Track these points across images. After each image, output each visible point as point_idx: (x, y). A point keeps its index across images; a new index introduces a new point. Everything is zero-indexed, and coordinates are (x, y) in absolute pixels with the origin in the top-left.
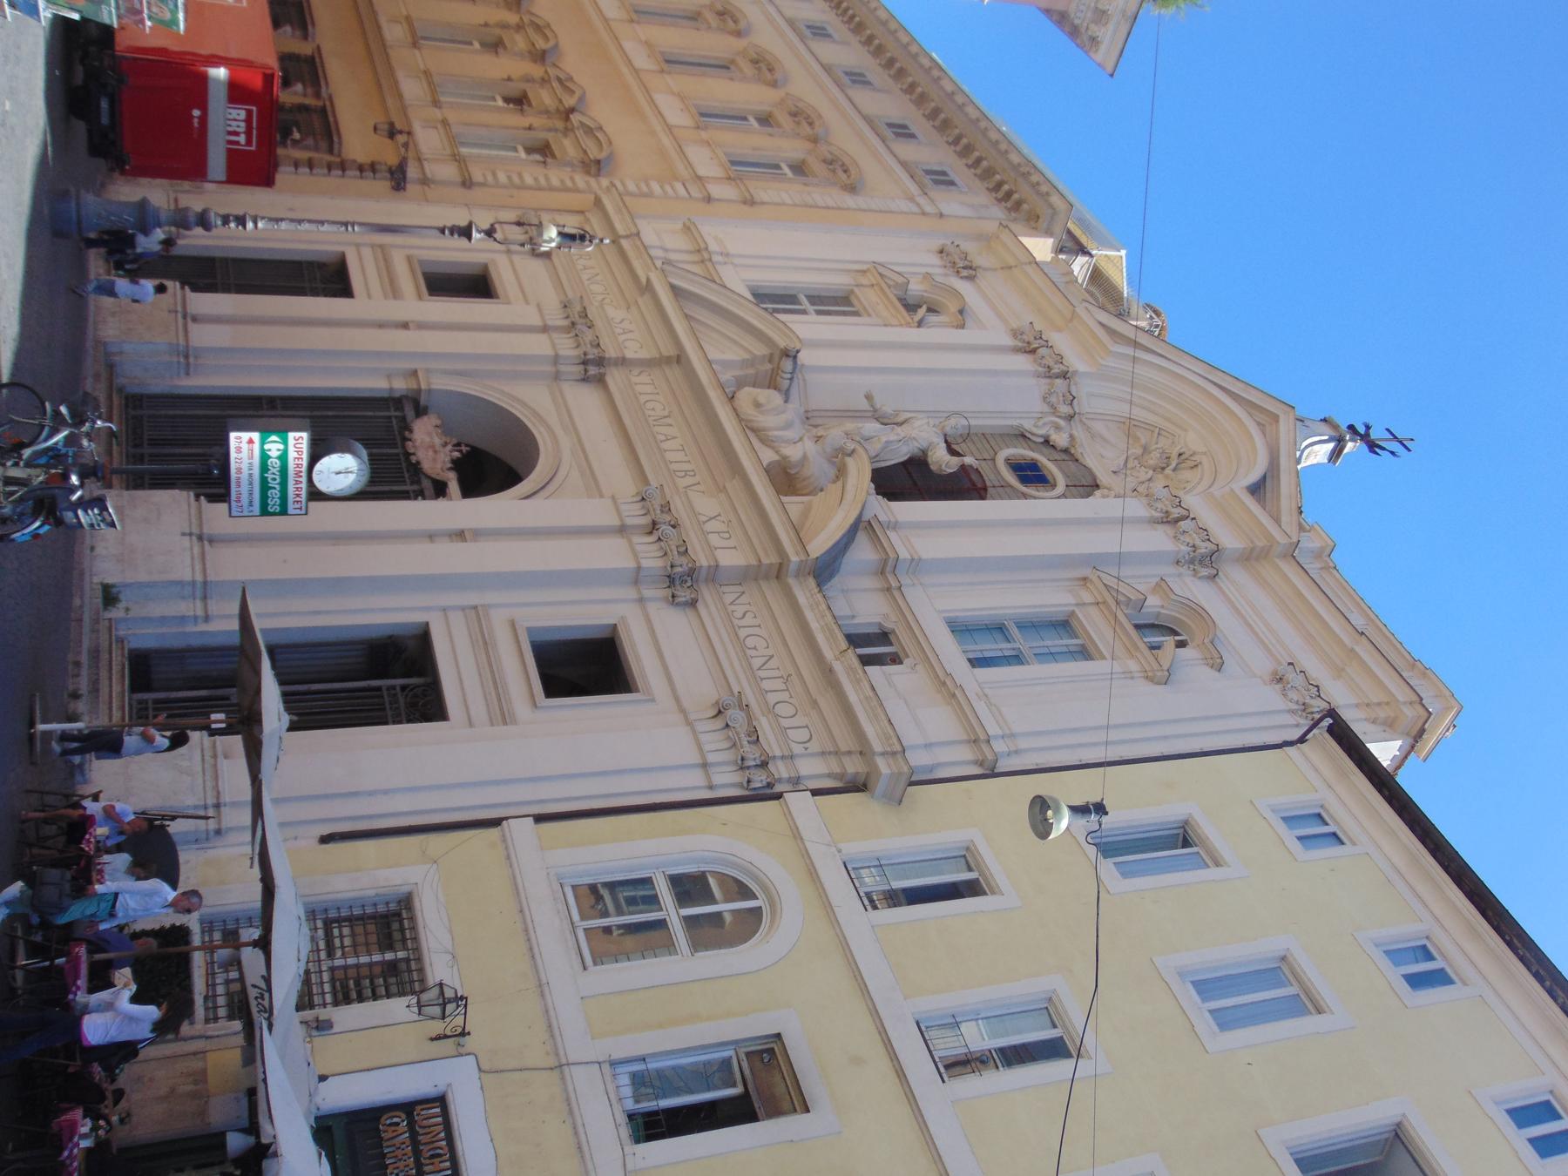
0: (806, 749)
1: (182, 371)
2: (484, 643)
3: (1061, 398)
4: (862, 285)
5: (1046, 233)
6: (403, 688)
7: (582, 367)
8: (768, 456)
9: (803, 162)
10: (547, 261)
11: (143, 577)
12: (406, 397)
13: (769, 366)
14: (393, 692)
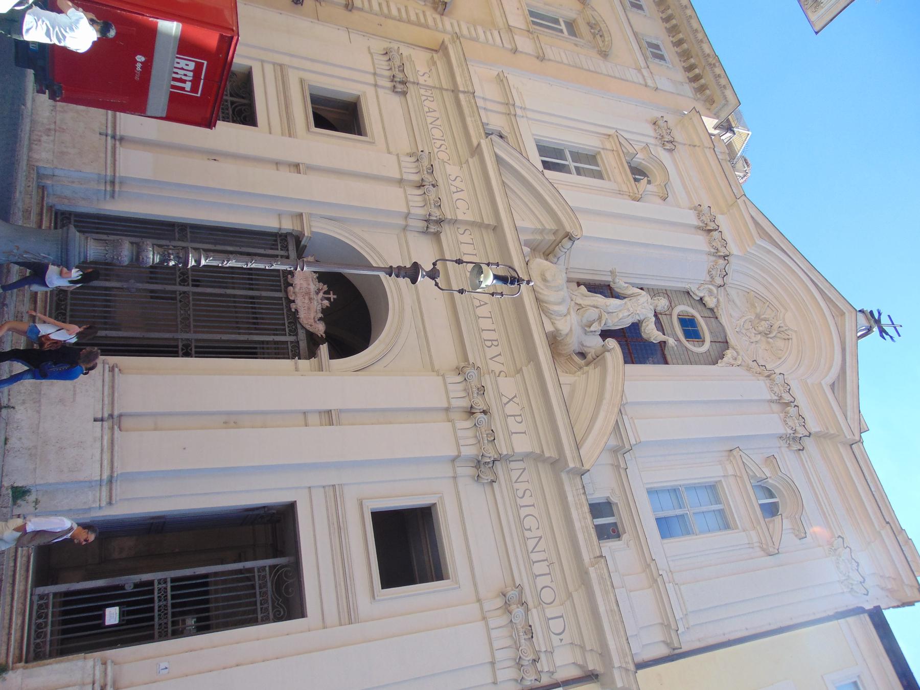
0: (561, 640)
1: (108, 196)
2: (339, 528)
3: (719, 273)
4: (607, 149)
5: (715, 114)
6: (272, 567)
7: (425, 224)
8: (549, 328)
9: (574, 21)
10: (403, 99)
11: (52, 478)
12: (290, 234)
13: (552, 238)
14: (263, 574)
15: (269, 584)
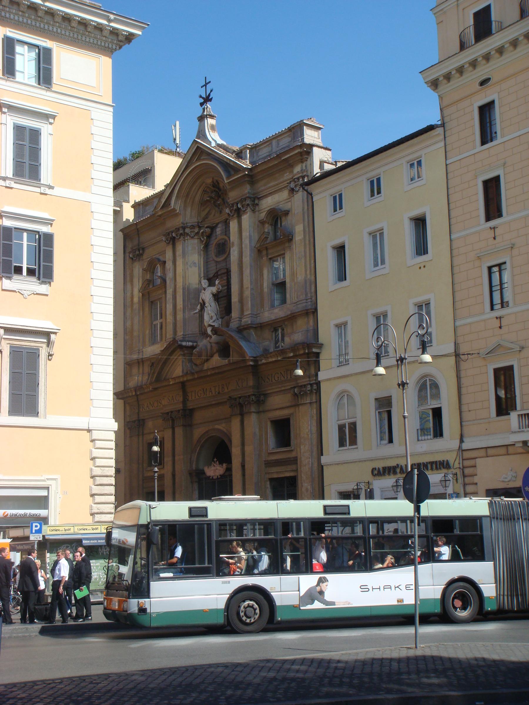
6: (287, 487)
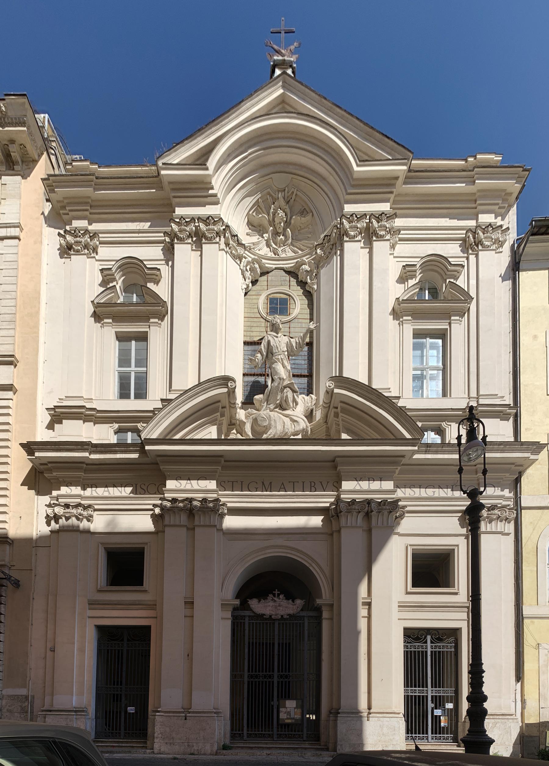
6: (432, 642)
15: (439, 644)
